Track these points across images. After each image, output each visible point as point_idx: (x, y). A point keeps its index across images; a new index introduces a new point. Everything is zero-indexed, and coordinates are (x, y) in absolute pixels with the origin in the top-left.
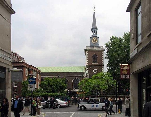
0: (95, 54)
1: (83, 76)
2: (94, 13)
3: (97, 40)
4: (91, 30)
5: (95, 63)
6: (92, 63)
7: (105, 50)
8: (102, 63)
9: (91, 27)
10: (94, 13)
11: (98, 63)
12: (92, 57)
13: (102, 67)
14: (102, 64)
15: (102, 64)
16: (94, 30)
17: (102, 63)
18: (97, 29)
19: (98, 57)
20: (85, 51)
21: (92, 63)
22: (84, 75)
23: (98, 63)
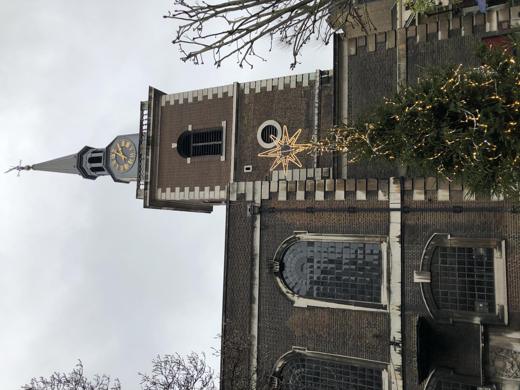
0: (174, 145)
1: (258, 201)
2: (35, 167)
3: (123, 142)
4: (94, 178)
5: (221, 140)
6: (223, 158)
7: (155, 89)
8: (225, 94)
9: (78, 178)
10: (35, 167)
11: (224, 124)
12: (189, 160)
13: (247, 91)
14: (230, 95)
15: (230, 95)
16: (90, 163)
17: (225, 94)
18: (87, 149)
19: (190, 128)
20: (153, 203)
21: (223, 158)
22: (249, 198)
23: (224, 124)
